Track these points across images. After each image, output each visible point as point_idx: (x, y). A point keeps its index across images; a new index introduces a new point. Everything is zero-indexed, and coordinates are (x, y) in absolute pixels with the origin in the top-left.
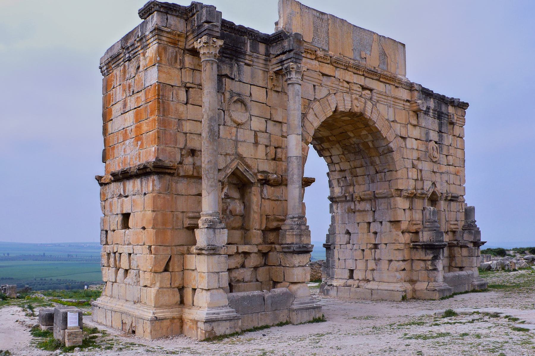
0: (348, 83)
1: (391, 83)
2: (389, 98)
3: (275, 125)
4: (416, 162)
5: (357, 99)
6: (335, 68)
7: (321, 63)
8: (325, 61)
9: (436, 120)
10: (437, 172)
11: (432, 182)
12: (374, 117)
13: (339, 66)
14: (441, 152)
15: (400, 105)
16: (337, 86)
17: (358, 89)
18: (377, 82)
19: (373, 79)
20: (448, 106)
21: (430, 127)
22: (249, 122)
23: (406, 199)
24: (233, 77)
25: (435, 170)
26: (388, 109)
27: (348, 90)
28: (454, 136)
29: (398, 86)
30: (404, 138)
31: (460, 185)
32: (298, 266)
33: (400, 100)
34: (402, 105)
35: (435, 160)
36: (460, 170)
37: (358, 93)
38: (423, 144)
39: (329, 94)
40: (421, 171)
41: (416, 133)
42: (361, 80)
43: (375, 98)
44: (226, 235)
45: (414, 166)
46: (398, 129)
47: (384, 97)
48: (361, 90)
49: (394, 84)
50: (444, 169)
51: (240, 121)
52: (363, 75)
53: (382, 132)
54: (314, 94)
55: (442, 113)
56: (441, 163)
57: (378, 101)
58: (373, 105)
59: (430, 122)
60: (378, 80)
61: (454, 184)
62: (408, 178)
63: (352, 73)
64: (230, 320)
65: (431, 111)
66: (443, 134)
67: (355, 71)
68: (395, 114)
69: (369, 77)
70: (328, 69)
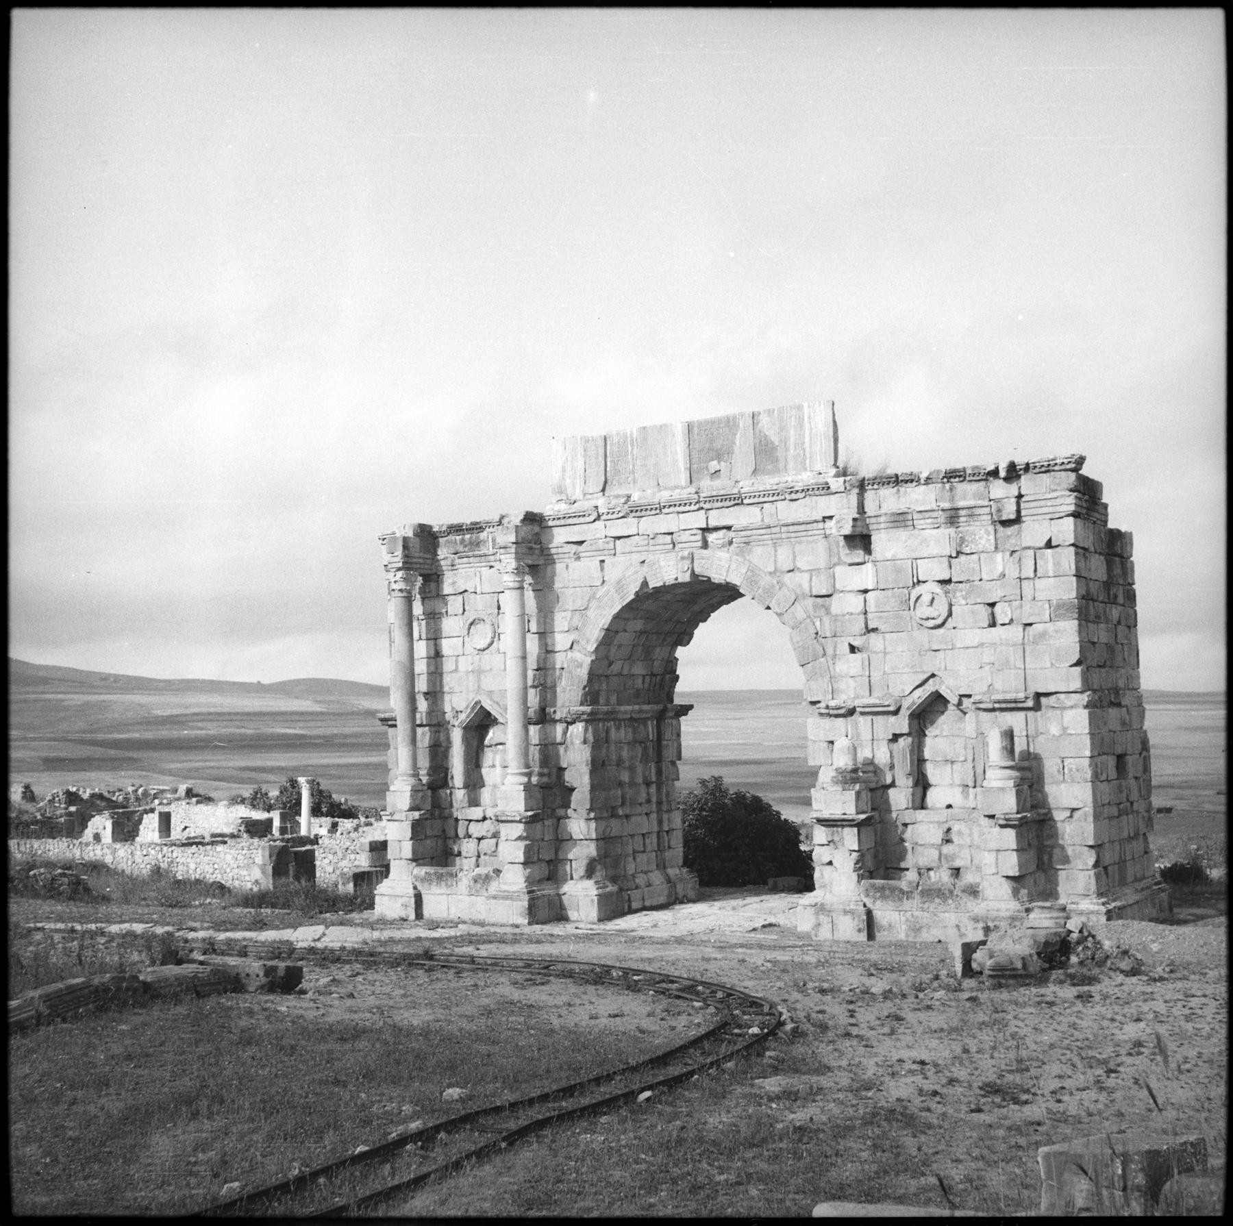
2: (774, 530)
5: (683, 558)
7: (608, 523)
8: (615, 516)
15: (810, 533)
17: (693, 538)
22: (495, 644)
26: (776, 551)
28: (1029, 548)
35: (931, 623)
41: (866, 576)
45: (853, 649)
51: (478, 648)
52: (702, 508)
54: (600, 574)
60: (742, 504)
67: (682, 509)
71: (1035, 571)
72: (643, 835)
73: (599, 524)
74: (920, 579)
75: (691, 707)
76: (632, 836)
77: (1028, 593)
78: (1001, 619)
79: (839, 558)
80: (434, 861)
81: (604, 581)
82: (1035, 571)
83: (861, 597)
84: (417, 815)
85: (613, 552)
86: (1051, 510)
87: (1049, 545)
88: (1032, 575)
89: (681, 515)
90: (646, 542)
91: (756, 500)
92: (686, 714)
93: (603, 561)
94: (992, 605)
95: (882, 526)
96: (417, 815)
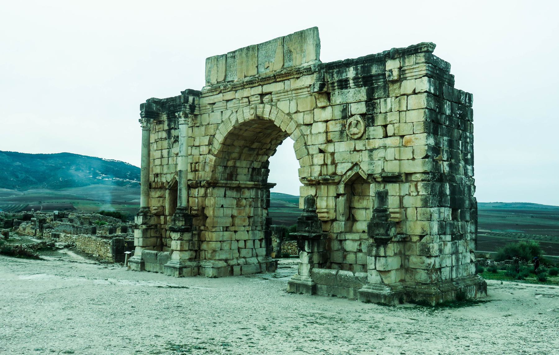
0: (248, 97)
1: (290, 77)
3: (196, 148)
4: (322, 147)
5: (252, 108)
6: (234, 92)
7: (224, 94)
8: (226, 91)
9: (363, 88)
10: (361, 150)
11: (352, 163)
12: (273, 117)
13: (237, 89)
14: (371, 124)
15: (304, 93)
16: (238, 105)
17: (256, 99)
18: (275, 84)
19: (270, 83)
20: (386, 61)
21: (349, 101)
23: (311, 187)
24: (176, 127)
25: (357, 149)
27: (248, 103)
29: (298, 76)
30: (311, 125)
31: (413, 159)
32: (175, 240)
33: (303, 88)
34: (307, 93)
35: (356, 137)
36: (413, 138)
37: (256, 102)
38: (337, 123)
39: (232, 113)
40: (333, 154)
41: (327, 114)
42: (258, 90)
43: (274, 98)
44: (142, 219)
46: (300, 118)
47: (283, 94)
48: (259, 96)
49: (293, 77)
50: (377, 143)
52: (260, 85)
53: (281, 127)
55: (372, 76)
56: (371, 137)
57: (279, 100)
58: (272, 105)
59: (351, 95)
60: (276, 82)
61: (395, 159)
62: (313, 165)
63: (250, 89)
64: (136, 263)
65: (351, 81)
66: (378, 101)
67: (251, 86)
68: (297, 105)
69: (265, 83)
70: (229, 95)
71: (407, 107)
72: (245, 241)
73: (221, 95)
74: (353, 113)
75: (275, 184)
76: (238, 241)
77: (403, 120)
78: (390, 132)
79: (316, 104)
80: (155, 248)
81: (222, 121)
82: (407, 107)
83: (325, 124)
84: (144, 227)
85: (226, 107)
86: (416, 73)
87: (414, 93)
88: (405, 109)
89: (252, 89)
90: (238, 102)
91: (282, 79)
92: (273, 187)
93: (222, 112)
94: (385, 126)
95: (336, 87)
96: (144, 227)
